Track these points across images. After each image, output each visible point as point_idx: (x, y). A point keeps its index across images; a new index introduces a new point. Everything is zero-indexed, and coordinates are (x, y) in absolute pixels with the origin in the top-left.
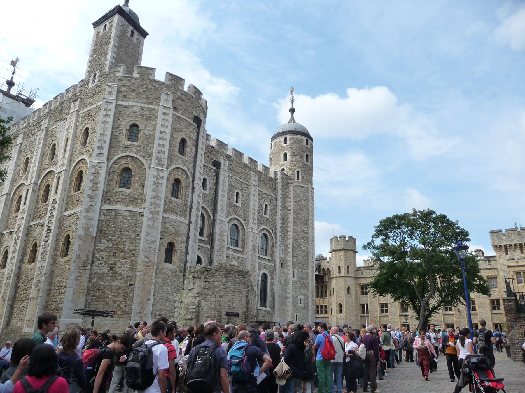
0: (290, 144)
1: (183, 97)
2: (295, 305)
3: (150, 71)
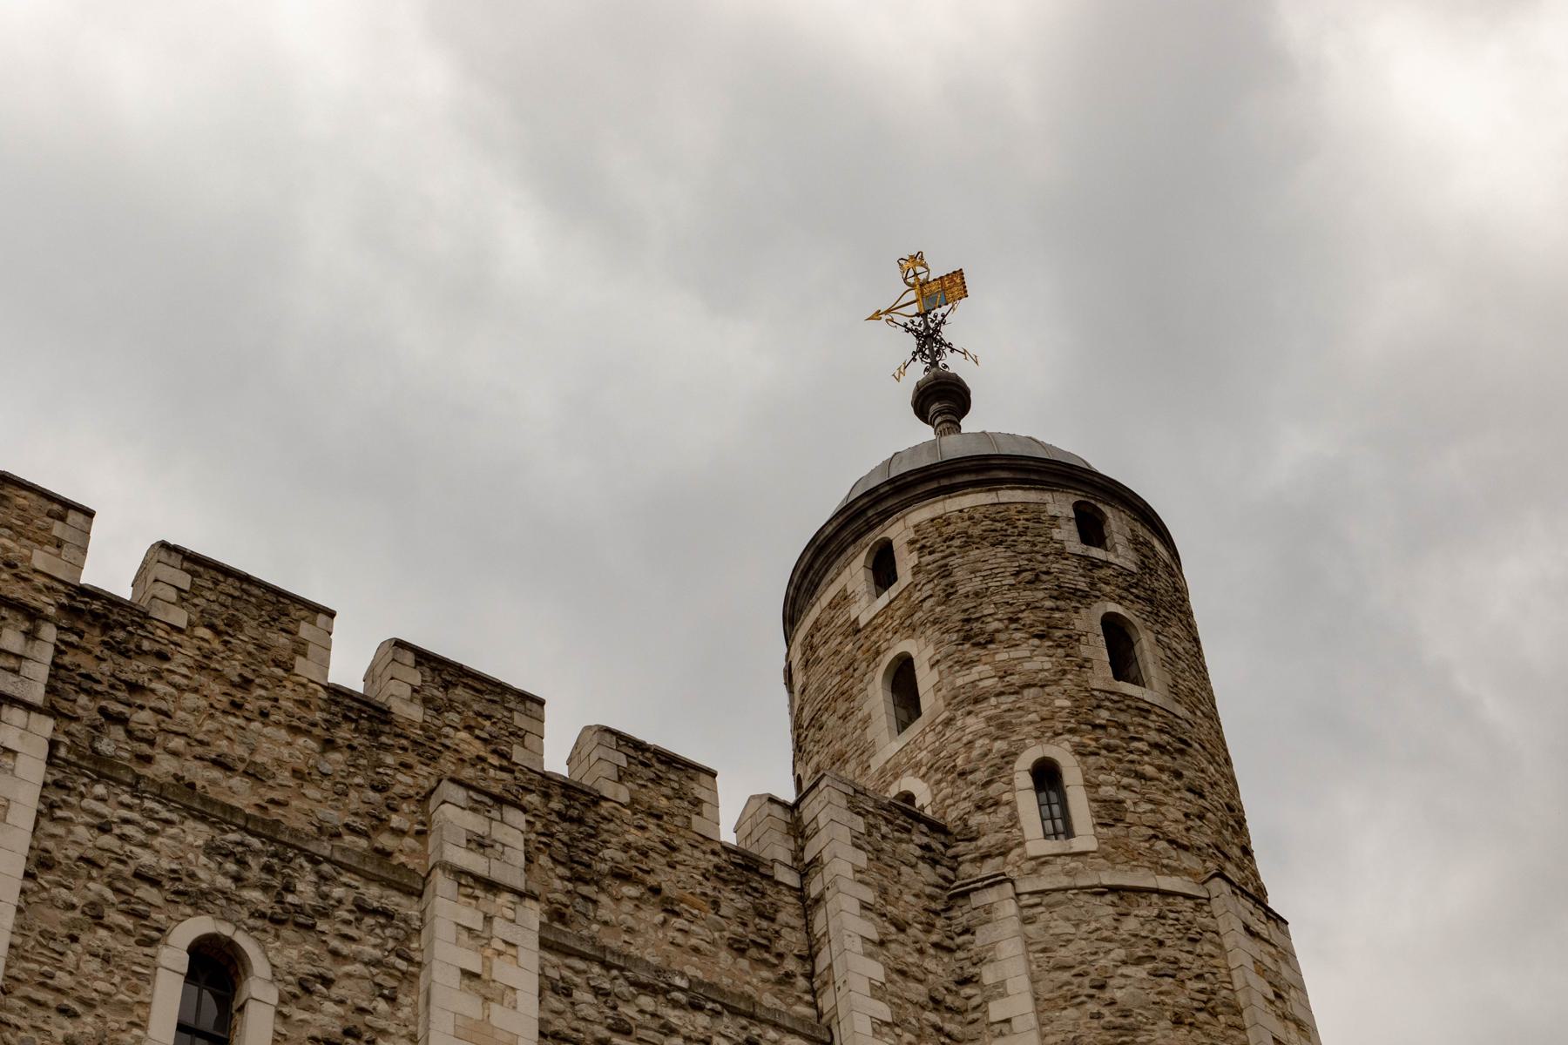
0: (917, 570)
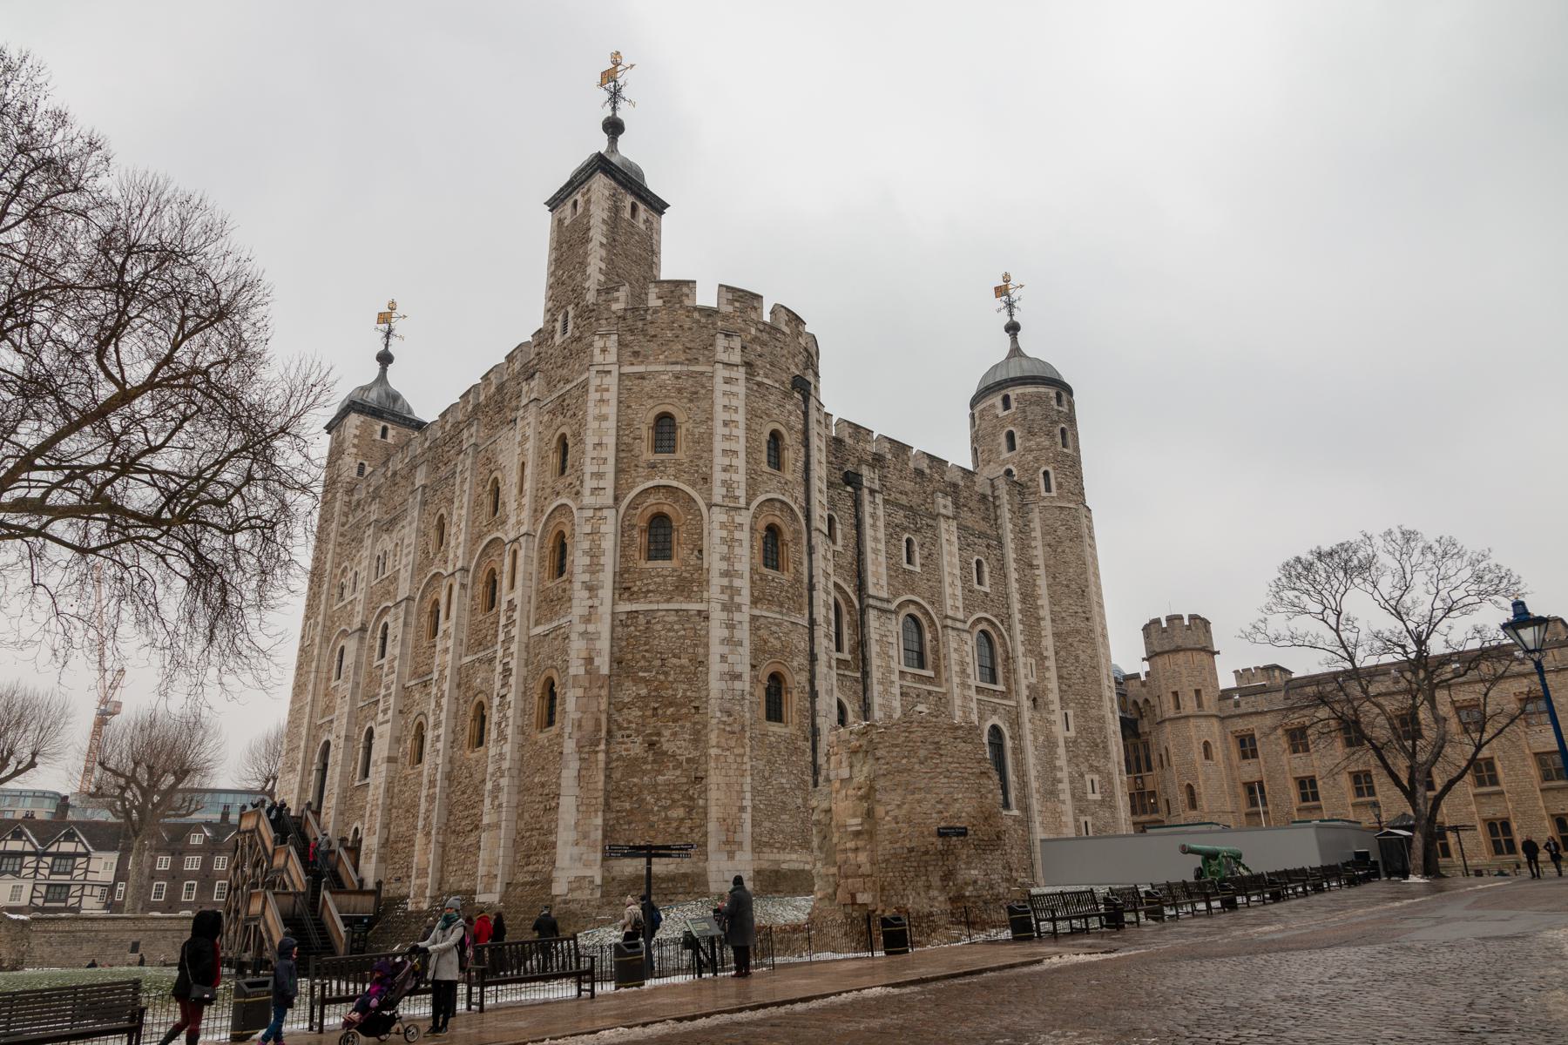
1: (765, 337)
2: (1078, 797)
3: (685, 290)
